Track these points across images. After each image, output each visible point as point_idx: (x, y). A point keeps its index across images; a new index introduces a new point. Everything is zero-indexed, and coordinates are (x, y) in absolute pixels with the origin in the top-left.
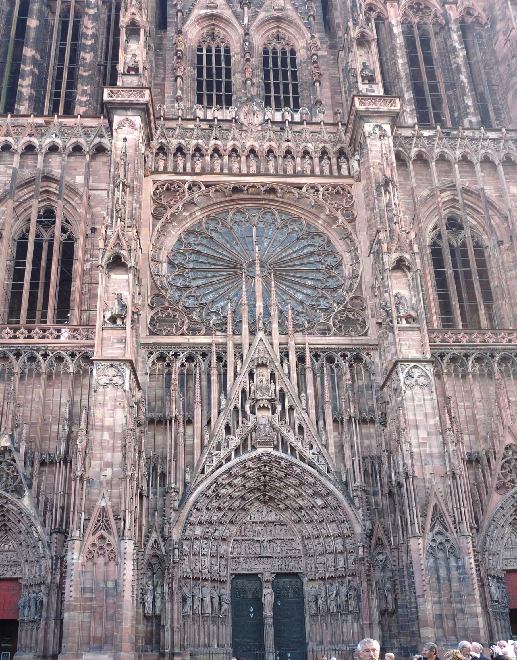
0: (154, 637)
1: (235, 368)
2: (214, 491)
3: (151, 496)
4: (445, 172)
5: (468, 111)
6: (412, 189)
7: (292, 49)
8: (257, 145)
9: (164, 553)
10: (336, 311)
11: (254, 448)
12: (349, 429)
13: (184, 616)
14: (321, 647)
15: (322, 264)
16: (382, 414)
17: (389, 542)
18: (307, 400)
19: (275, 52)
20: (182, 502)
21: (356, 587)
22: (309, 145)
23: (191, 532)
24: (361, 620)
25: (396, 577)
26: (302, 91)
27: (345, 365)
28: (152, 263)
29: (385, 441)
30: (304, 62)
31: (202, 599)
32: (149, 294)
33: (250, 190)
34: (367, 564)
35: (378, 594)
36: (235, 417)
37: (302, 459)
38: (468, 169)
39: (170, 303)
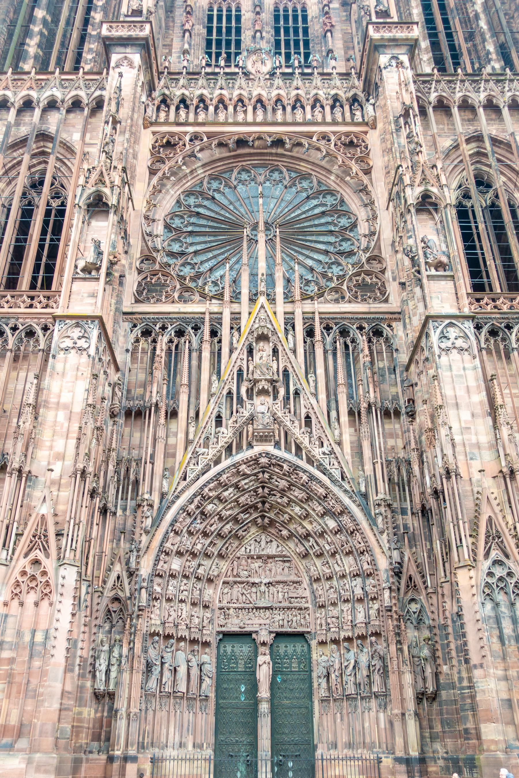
0: (104, 728)
1: (231, 344)
2: (198, 507)
3: (119, 512)
4: (469, 120)
5: (490, 56)
6: (433, 136)
7: (304, 7)
8: (264, 93)
9: (128, 595)
10: (350, 273)
11: (250, 446)
12: (368, 422)
13: (148, 696)
14: (333, 753)
15: (335, 225)
16: (409, 400)
17: (424, 583)
18: (316, 381)
19: (286, 10)
20: (157, 522)
21: (382, 653)
22: (320, 92)
23: (166, 566)
24: (389, 708)
25: (437, 638)
26: (313, 47)
27: (362, 340)
28: (143, 221)
29: (415, 437)
30: (316, 17)
31: (175, 668)
32: (139, 255)
33: (257, 143)
34: (395, 616)
35: (413, 665)
36: (228, 406)
37: (310, 461)
38: (493, 116)
39: (161, 266)
